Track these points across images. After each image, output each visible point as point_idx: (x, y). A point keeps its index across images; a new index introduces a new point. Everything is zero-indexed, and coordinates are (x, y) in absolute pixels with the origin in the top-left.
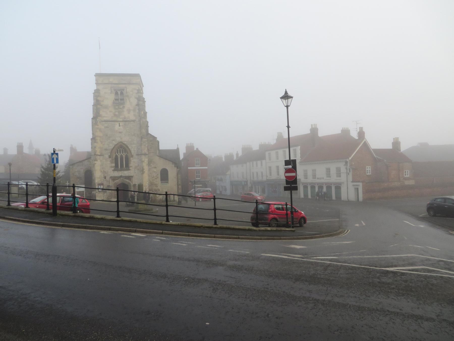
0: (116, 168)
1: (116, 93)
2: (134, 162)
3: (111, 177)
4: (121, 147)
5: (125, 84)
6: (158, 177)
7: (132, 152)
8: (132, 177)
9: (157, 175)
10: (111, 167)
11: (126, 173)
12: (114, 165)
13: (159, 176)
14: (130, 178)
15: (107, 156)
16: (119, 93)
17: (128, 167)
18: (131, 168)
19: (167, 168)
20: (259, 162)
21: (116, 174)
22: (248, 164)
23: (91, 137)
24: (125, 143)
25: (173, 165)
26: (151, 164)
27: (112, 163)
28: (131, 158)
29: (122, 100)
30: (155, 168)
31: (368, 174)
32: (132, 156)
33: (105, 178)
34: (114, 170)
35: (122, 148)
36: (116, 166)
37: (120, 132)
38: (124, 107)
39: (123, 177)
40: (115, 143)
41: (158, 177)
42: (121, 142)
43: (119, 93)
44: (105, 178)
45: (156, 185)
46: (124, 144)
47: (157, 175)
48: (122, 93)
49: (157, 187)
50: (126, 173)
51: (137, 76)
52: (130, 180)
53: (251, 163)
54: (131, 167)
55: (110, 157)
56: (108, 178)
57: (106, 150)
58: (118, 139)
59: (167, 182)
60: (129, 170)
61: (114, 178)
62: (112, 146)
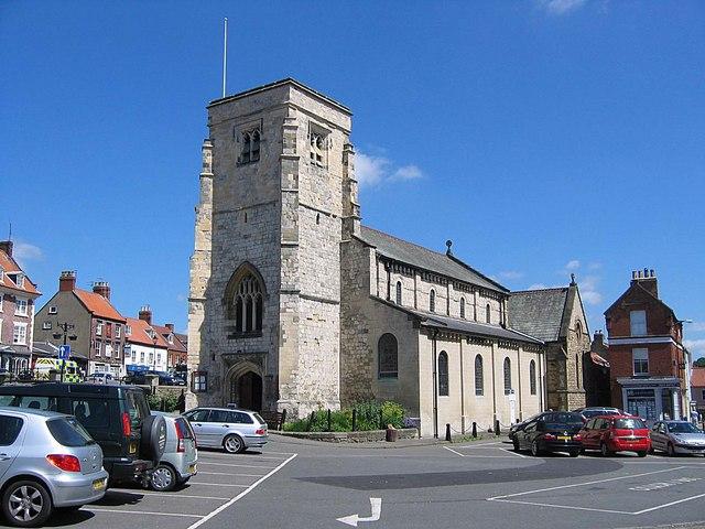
0: (237, 333)
1: (247, 140)
5: (260, 111)
10: (230, 328)
29: (256, 152)
30: (366, 331)
34: (229, 337)
37: (245, 237)
38: (256, 170)
39: (246, 354)
41: (371, 360)
48: (257, 138)
49: (369, 387)
50: (252, 344)
52: (259, 362)
58: (242, 255)
60: (261, 335)
62: (229, 273)
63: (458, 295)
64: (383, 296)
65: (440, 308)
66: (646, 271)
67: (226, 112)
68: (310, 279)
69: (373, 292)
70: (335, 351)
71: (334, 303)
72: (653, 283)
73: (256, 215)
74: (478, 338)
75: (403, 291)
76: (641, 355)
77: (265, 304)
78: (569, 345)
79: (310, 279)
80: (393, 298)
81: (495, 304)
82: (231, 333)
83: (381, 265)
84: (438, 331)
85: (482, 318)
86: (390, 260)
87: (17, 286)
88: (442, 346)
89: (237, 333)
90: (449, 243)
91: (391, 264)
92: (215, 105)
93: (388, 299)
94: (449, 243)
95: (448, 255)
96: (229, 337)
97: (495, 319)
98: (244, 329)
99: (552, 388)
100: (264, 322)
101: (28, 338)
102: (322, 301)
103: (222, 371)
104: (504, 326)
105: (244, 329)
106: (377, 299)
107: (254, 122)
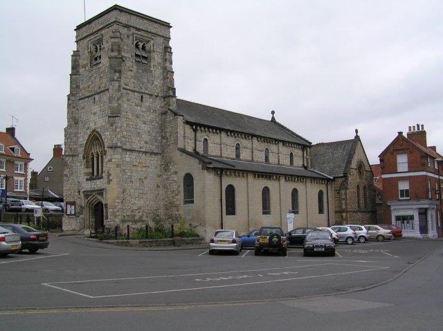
3: (83, 192)
6: (179, 192)
8: (103, 189)
9: (179, 186)
10: (87, 174)
11: (98, 184)
12: (91, 170)
13: (182, 189)
14: (101, 192)
15: (81, 156)
21: (88, 186)
24: (99, 130)
26: (171, 167)
30: (176, 173)
34: (87, 180)
41: (179, 192)
46: (97, 132)
47: (179, 186)
50: (98, 184)
55: (84, 158)
58: (92, 126)
60: (102, 178)
61: (87, 194)
63: (264, 146)
64: (190, 149)
65: (273, 159)
66: (418, 126)
67: (85, 32)
68: (135, 140)
69: (181, 145)
70: (158, 186)
71: (156, 154)
72: (423, 134)
73: (100, 98)
74: (290, 177)
75: (210, 145)
76: (404, 186)
77: (104, 157)
78: (350, 179)
79: (135, 140)
80: (200, 149)
81: (298, 152)
82: (88, 177)
83: (188, 127)
84: (221, 169)
85: (285, 161)
86: (197, 125)
87: (15, 155)
88: (227, 181)
89: (92, 177)
90: (273, 113)
91: (195, 126)
93: (195, 150)
94: (273, 113)
95: (273, 118)
96: (87, 180)
97: (298, 162)
98: (95, 174)
99: (338, 209)
101: (25, 187)
102: (146, 153)
103: (83, 201)
104: (306, 168)
105: (95, 174)
106: (183, 151)
107: (98, 36)
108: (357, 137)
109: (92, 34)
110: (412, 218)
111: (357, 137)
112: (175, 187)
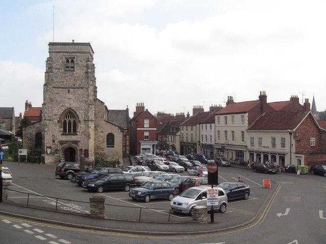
0: (64, 133)
1: (68, 61)
2: (81, 127)
3: (59, 141)
4: (70, 112)
7: (80, 117)
11: (73, 138)
12: (62, 129)
13: (106, 140)
14: (76, 142)
16: (70, 61)
17: (75, 133)
18: (78, 133)
19: (113, 132)
20: (208, 125)
21: (64, 138)
22: (198, 126)
23: (43, 103)
24: (74, 109)
25: (120, 130)
27: (60, 127)
28: (79, 124)
29: (73, 67)
30: (102, 132)
31: (313, 145)
32: (80, 122)
33: (54, 141)
34: (62, 135)
35: (70, 113)
36: (65, 130)
39: (70, 141)
40: (64, 109)
42: (70, 108)
43: (70, 61)
44: (54, 141)
45: (102, 149)
46: (73, 110)
48: (72, 61)
50: (73, 138)
51: (88, 45)
53: (201, 125)
54: (79, 132)
55: (59, 122)
56: (56, 142)
57: (55, 115)
58: (67, 105)
59: (113, 147)
60: (77, 135)
61: (62, 143)
76: (146, 134)
89: (64, 133)
92: (50, 44)
96: (62, 135)
100: (78, 130)
108: (127, 109)
109: (66, 52)
110: (149, 149)
111: (127, 109)
112: (101, 139)
